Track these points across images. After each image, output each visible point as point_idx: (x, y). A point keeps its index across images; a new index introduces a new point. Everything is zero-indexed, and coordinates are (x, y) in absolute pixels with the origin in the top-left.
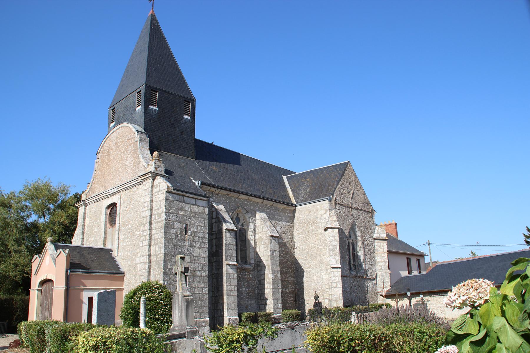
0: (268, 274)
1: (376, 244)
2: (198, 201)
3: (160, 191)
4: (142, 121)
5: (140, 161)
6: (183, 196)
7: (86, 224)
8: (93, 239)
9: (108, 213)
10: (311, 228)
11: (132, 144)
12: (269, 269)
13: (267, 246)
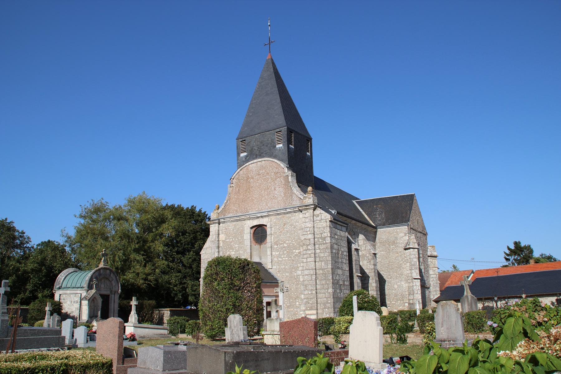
0: (371, 283)
1: (429, 260)
3: (321, 220)
4: (286, 157)
5: (292, 193)
6: (336, 223)
12: (373, 279)
13: (370, 262)
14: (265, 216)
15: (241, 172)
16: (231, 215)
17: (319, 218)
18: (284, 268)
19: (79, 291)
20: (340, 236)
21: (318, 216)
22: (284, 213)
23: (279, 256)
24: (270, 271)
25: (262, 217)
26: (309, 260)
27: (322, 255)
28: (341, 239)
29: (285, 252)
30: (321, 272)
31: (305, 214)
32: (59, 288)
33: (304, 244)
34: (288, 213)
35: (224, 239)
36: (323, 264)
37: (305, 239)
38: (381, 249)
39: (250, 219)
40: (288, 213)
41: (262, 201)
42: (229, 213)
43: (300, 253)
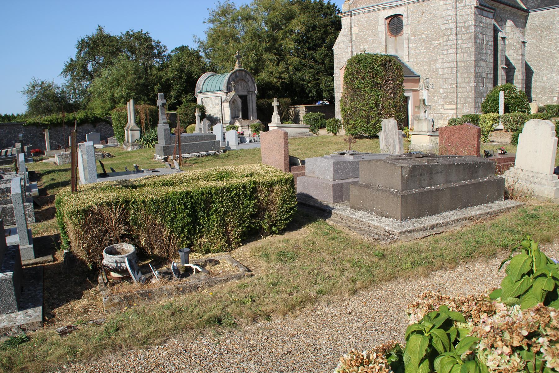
0: (517, 76)
2: (484, 12)
3: (466, 6)
6: (483, 9)
7: (353, 33)
9: (387, 24)
10: (545, 33)
12: (519, 71)
13: (517, 51)
14: (401, 5)
16: (364, 6)
18: (422, 61)
19: (219, 94)
20: (487, 24)
23: (416, 48)
24: (407, 64)
25: (397, 6)
26: (449, 52)
27: (464, 46)
28: (487, 28)
29: (423, 44)
30: (463, 64)
32: (200, 92)
33: (444, 35)
35: (357, 32)
36: (465, 55)
37: (446, 29)
38: (531, 36)
39: (384, 9)
43: (439, 44)
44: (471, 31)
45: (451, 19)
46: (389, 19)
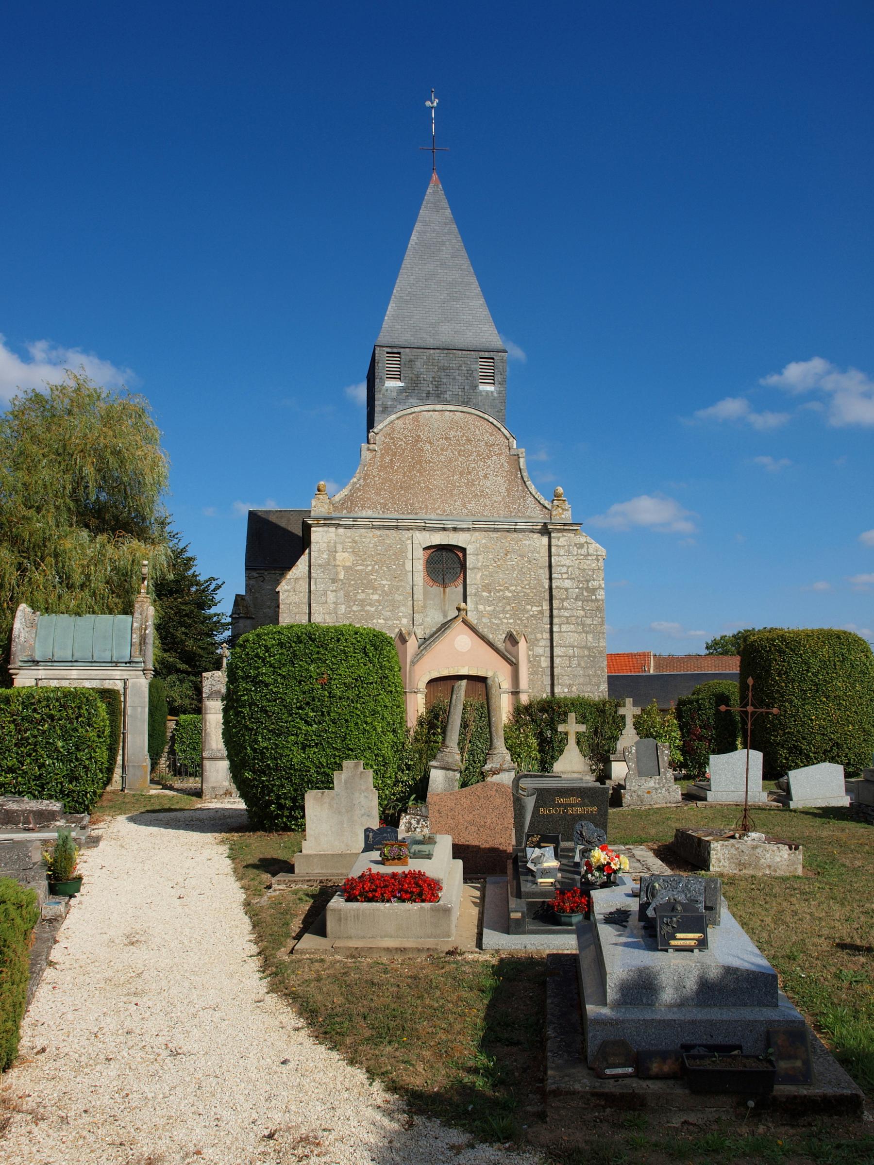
3: (588, 555)
8: (376, 597)
11: (501, 454)
14: (462, 530)
15: (399, 423)
16: (370, 513)
17: (583, 551)
21: (581, 546)
22: (508, 531)
23: (493, 615)
25: (455, 529)
26: (564, 628)
27: (588, 621)
30: (586, 653)
31: (559, 538)
34: (515, 530)
35: (348, 564)
36: (590, 637)
40: (515, 530)
41: (452, 496)
42: (363, 507)
44: (599, 597)
45: (567, 573)
46: (429, 552)
